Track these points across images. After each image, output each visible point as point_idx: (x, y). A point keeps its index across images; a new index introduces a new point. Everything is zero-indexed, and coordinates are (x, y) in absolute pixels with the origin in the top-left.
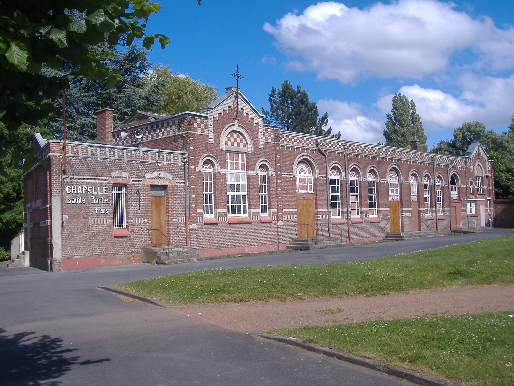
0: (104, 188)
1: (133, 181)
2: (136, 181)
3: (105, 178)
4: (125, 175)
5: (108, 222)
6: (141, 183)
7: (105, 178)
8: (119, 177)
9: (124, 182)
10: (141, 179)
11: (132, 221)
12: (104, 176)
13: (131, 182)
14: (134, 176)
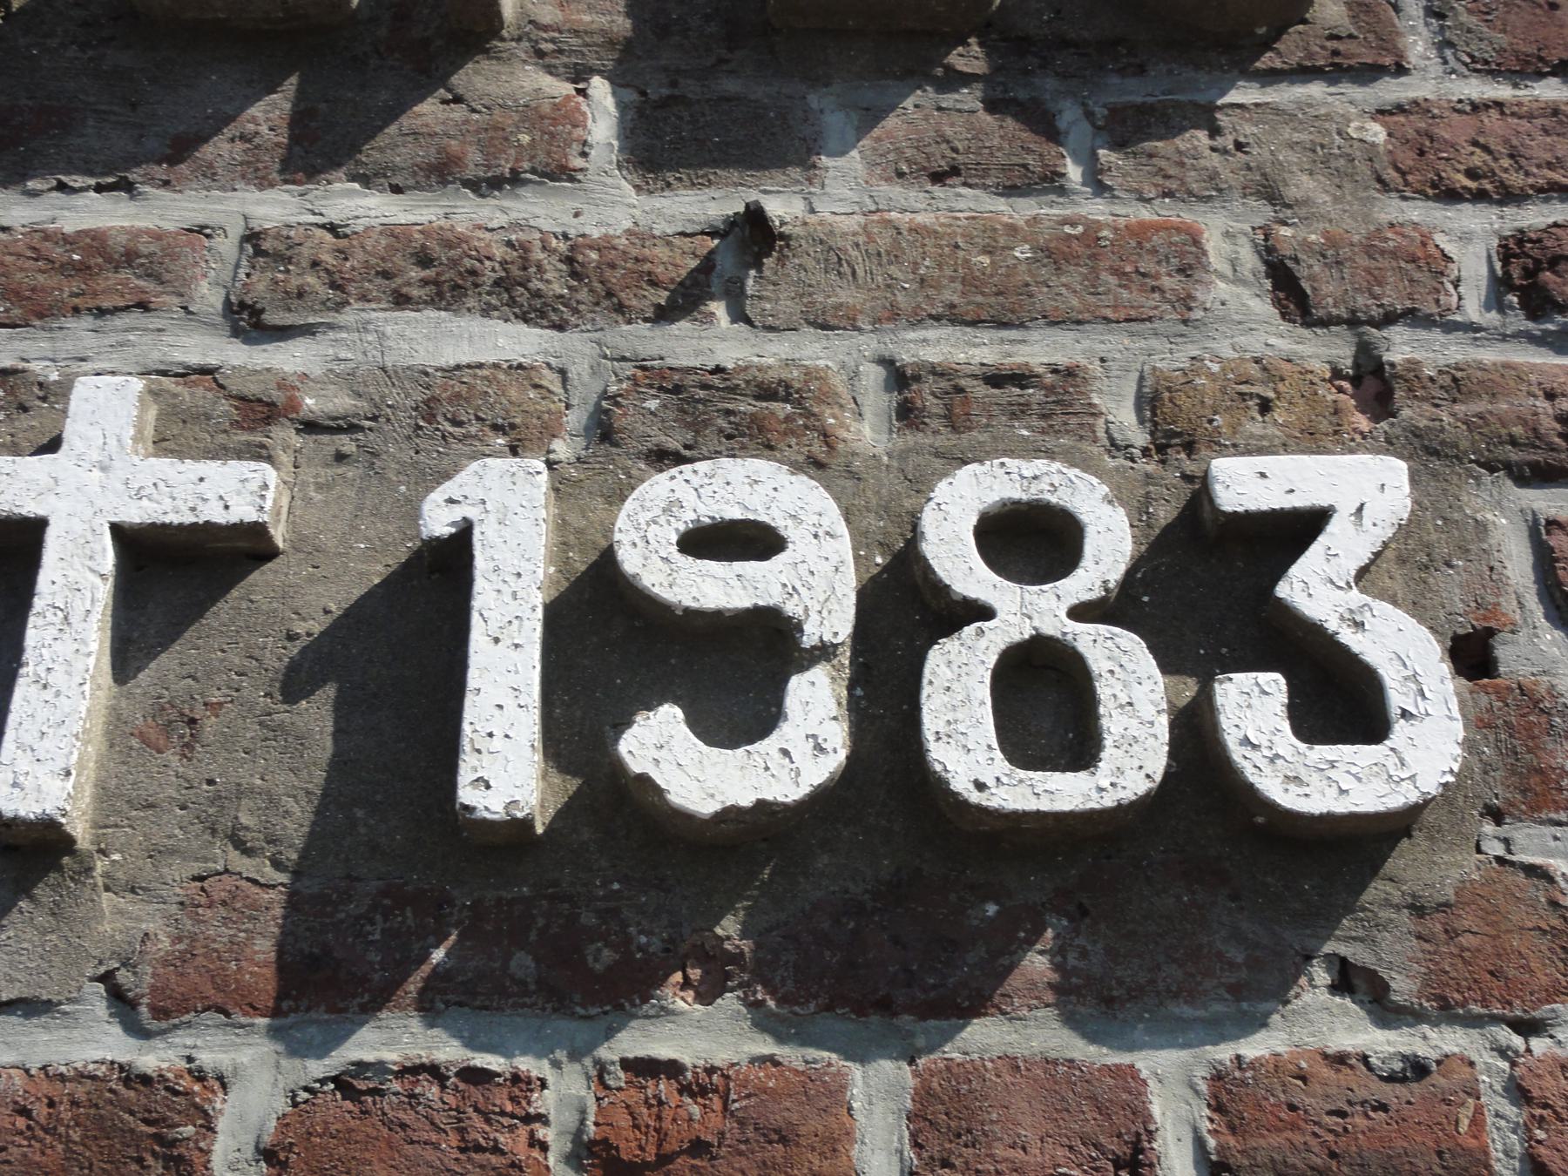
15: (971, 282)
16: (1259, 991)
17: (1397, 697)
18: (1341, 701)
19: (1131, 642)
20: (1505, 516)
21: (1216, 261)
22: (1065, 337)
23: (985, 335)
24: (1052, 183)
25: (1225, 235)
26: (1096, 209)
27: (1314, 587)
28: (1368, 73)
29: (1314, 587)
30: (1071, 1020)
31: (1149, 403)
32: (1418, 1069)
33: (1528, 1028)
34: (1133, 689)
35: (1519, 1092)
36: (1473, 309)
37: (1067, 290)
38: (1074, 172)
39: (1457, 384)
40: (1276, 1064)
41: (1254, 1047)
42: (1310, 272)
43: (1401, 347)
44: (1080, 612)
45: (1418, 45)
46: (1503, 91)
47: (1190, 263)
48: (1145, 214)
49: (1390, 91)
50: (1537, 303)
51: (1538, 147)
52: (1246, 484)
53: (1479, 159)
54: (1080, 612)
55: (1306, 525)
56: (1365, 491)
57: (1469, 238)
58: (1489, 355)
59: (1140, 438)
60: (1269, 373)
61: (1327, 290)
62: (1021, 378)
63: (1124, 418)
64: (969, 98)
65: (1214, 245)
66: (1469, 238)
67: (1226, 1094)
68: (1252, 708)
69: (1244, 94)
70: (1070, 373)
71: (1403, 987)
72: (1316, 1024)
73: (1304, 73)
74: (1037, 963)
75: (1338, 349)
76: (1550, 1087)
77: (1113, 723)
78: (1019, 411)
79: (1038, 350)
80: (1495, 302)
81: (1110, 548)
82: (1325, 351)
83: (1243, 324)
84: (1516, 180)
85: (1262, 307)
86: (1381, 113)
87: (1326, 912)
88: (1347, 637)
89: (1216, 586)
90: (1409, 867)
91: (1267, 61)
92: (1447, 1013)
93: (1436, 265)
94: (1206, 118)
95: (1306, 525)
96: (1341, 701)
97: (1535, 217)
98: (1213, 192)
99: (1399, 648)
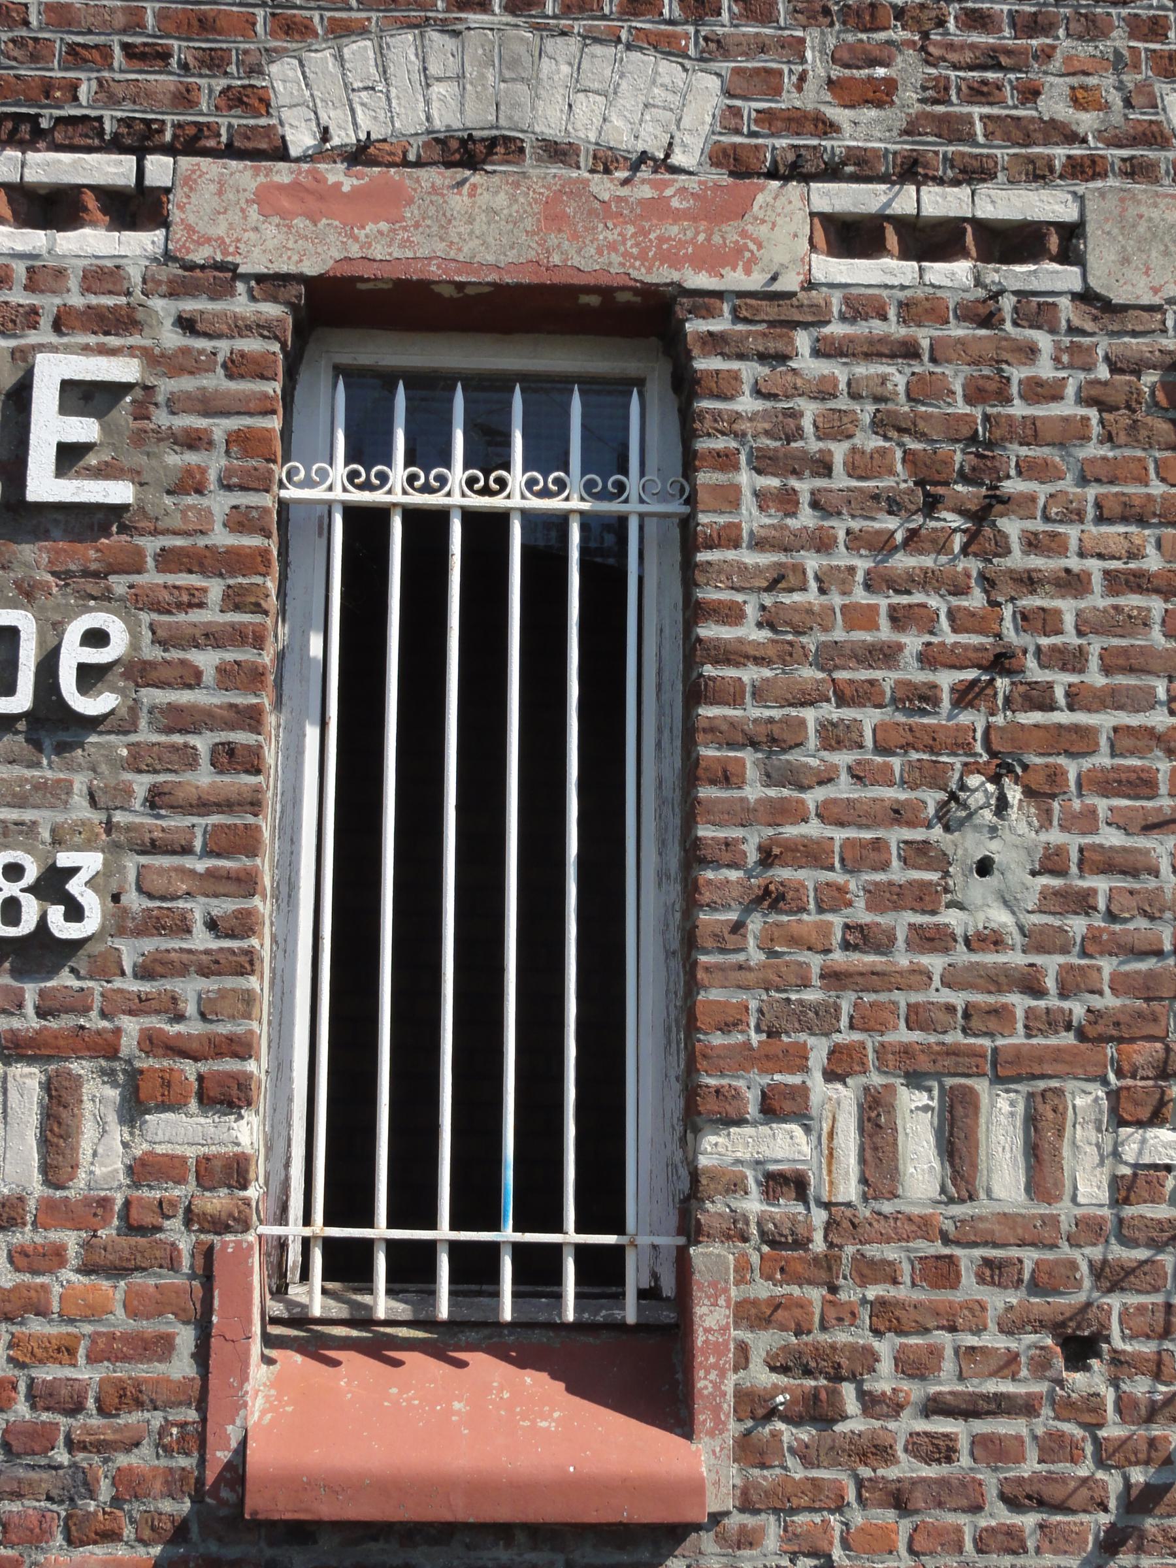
0: (52, 371)
1: (851, 236)
2: (930, 240)
3: (114, 170)
4: (651, 102)
5: (104, 1153)
6: (1053, 277)
7: (114, 170)
8: (466, 152)
9: (600, 253)
10: (1050, 205)
11: (787, 1145)
12: (82, 134)
13: (781, 237)
14: (861, 129)
15: (14, 795)
16: (53, 972)
17: (87, 913)
18: (75, 912)
19: (31, 897)
20: (131, 863)
21: (76, 790)
22: (36, 811)
23: (16, 810)
24: (37, 765)
25: (80, 783)
26: (49, 774)
27: (75, 886)
28: (126, 733)
29: (75, 886)
30: (13, 977)
31: (53, 831)
32: (82, 989)
33: (108, 982)
34: (30, 908)
35: (102, 995)
36: (137, 807)
37: (37, 798)
38: (45, 762)
39: (129, 828)
40: (53, 988)
41: (49, 984)
42: (99, 795)
43: (119, 817)
44: (22, 890)
45: (143, 723)
46: (163, 738)
47: (69, 792)
48: (62, 776)
49: (133, 738)
50: (153, 806)
51: (166, 756)
52: (64, 859)
53: (150, 761)
54: (22, 890)
55: (74, 871)
56: (90, 862)
57: (141, 784)
58: (138, 820)
59: (49, 840)
60: (83, 824)
61: (102, 800)
62: (22, 824)
63: (46, 835)
64: (21, 738)
65: (76, 787)
66: (141, 784)
67: (42, 993)
68: (56, 913)
69: (93, 739)
70: (34, 823)
71: (83, 972)
72: (65, 979)
73: (109, 732)
74: (7, 965)
75: (104, 818)
76: (109, 995)
77: (24, 917)
78: (21, 833)
79: (28, 815)
80: (143, 805)
81: (32, 873)
82: (97, 817)
83: (80, 809)
84: (158, 767)
85: (85, 803)
86: (128, 746)
87: (69, 957)
88: (80, 899)
89: (53, 885)
90: (89, 948)
91: (101, 728)
92: (91, 978)
93: (129, 793)
94: (81, 745)
95: (74, 871)
96: (75, 912)
97: (161, 778)
98: (78, 769)
99: (91, 901)
